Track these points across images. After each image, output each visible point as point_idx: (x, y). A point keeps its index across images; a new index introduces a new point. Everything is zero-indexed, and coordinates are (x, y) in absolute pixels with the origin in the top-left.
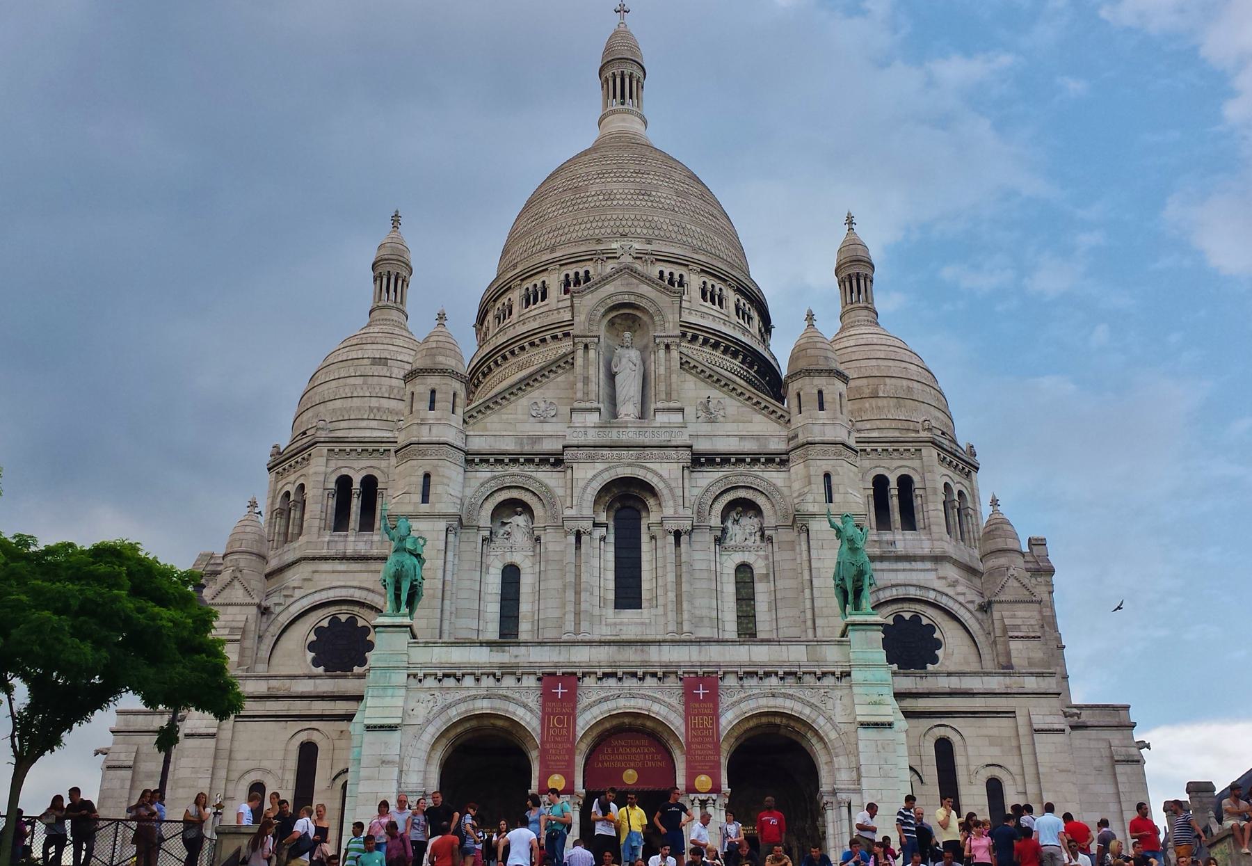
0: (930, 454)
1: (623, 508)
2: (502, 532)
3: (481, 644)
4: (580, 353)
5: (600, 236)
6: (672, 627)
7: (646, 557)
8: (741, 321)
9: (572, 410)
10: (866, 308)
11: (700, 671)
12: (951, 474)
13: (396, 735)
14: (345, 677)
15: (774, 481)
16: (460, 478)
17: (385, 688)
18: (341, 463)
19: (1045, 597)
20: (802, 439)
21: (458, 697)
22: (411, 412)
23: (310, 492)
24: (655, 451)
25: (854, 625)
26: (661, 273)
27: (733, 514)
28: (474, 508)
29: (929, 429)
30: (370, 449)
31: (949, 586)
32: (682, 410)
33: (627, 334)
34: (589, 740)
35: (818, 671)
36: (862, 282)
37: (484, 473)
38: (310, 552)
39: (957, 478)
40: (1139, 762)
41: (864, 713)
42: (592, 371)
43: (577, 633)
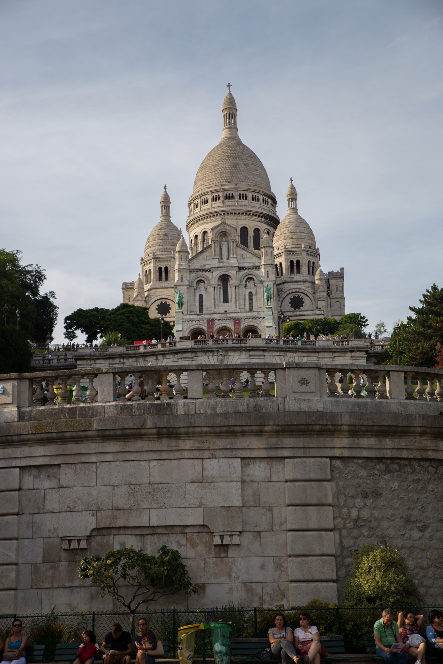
0: (304, 254)
3: (196, 315)
6: (234, 307)
8: (265, 205)
18: (159, 264)
19: (341, 285)
21: (192, 324)
23: (152, 271)
26: (240, 194)
29: (305, 247)
32: (236, 258)
33: (224, 239)
37: (194, 274)
38: (154, 287)
39: (313, 258)
41: (267, 324)
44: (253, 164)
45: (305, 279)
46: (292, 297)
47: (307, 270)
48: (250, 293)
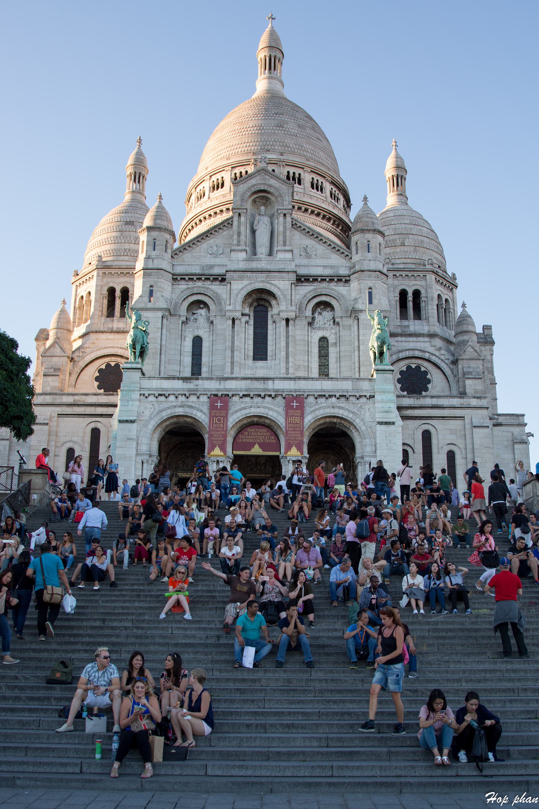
0: (431, 277)
1: (259, 305)
2: (192, 318)
3: (178, 379)
4: (236, 219)
5: (255, 151)
6: (283, 370)
7: (270, 332)
8: (333, 201)
9: (231, 251)
10: (401, 195)
11: (295, 395)
12: (442, 289)
13: (135, 425)
14: (113, 395)
15: (341, 292)
16: (170, 288)
17: (128, 401)
18: (109, 280)
20: (357, 268)
21: (166, 405)
22: (142, 252)
24: (276, 274)
25: (377, 370)
26: (288, 172)
27: (319, 310)
28: (177, 306)
29: (432, 264)
30: (125, 272)
31: (437, 350)
32: (292, 251)
33: (263, 208)
34: (235, 429)
35: (358, 395)
36: (399, 180)
37: (183, 286)
38: (94, 329)
40: (525, 443)
41: (380, 417)
42: (242, 229)
43: (232, 373)
44: (313, 129)
45: (432, 332)
46: (404, 369)
47: (436, 312)
48: (323, 340)
